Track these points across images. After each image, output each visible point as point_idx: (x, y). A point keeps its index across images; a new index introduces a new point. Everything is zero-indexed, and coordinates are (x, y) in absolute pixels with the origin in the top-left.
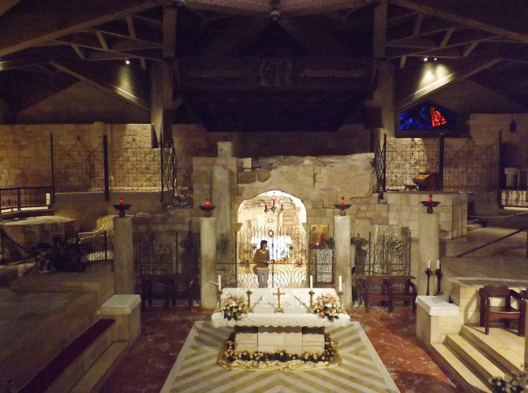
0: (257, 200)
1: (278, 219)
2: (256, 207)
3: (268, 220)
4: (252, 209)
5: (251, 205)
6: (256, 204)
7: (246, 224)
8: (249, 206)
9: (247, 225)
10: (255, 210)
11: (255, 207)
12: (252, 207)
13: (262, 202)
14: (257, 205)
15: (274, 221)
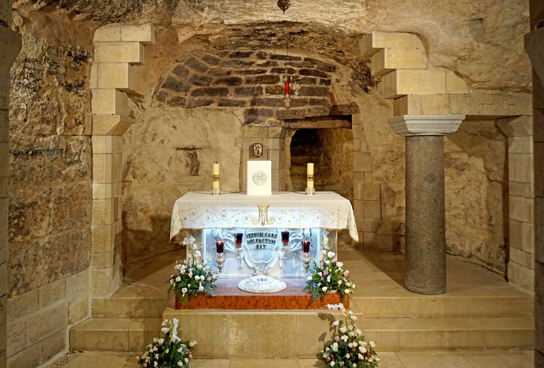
0: (215, 78)
1: (282, 149)
2: (212, 106)
3: (252, 148)
4: (199, 111)
5: (195, 93)
6: (212, 92)
7: (184, 161)
8: (188, 97)
9: (187, 165)
10: (211, 115)
11: (209, 103)
12: (199, 104)
13: (232, 89)
14: (216, 98)
15: (271, 153)
